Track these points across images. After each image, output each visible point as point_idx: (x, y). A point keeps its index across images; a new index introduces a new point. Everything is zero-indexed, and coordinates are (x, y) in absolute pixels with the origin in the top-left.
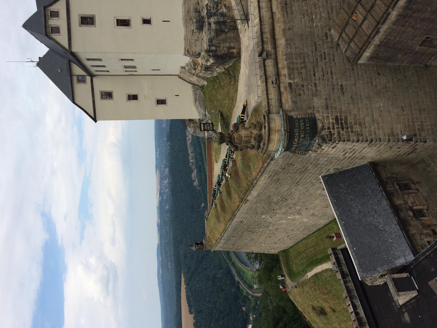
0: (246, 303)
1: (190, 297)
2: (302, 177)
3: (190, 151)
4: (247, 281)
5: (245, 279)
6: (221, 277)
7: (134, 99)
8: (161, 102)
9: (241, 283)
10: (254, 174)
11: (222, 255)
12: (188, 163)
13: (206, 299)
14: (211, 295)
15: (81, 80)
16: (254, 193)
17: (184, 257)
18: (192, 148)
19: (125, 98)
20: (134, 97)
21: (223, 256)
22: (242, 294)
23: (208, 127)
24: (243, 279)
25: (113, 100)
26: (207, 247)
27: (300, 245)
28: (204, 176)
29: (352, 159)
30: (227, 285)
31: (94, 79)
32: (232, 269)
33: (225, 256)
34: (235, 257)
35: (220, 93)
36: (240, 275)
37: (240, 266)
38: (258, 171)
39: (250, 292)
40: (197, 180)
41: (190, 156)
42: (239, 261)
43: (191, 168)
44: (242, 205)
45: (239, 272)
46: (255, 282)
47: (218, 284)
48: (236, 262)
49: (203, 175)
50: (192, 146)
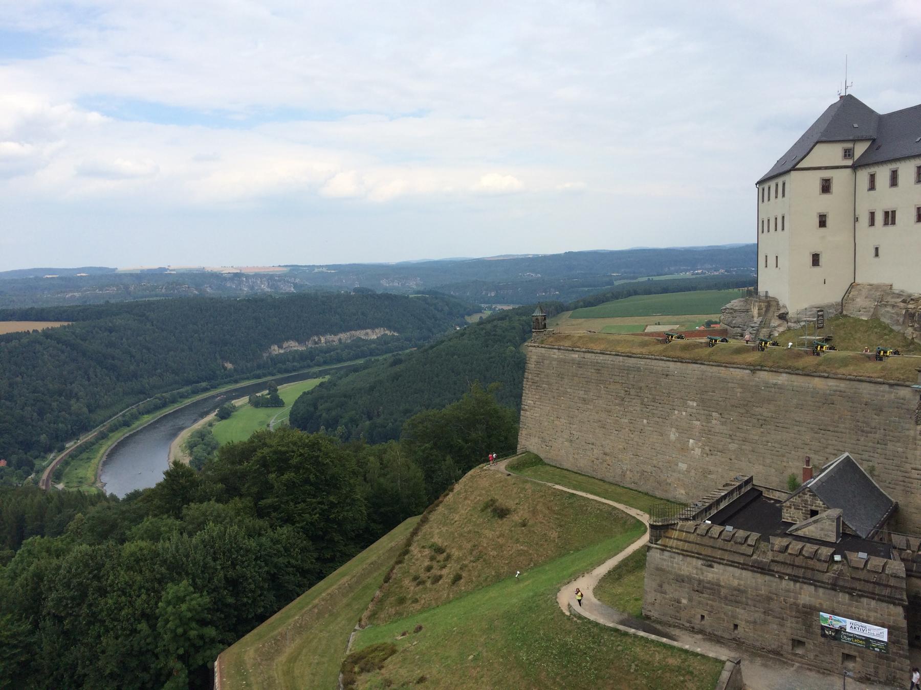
0: (19, 466)
1: (20, 341)
2: (841, 432)
3: (343, 336)
4: (69, 468)
5: (72, 464)
6: (70, 409)
7: (820, 222)
8: (816, 260)
9: (63, 455)
10: (842, 370)
11: (121, 411)
12: (317, 334)
13: (18, 376)
14: (28, 389)
15: (848, 154)
16: (782, 379)
17: (110, 327)
18: (349, 341)
19: (823, 211)
20: (823, 223)
21: (117, 413)
22: (36, 457)
23: (820, 322)
24: (73, 459)
25: (820, 194)
26: (542, 334)
27: (580, 477)
28: (294, 366)
29: (904, 481)
30: (54, 423)
31: (849, 171)
32: (90, 433)
33: (120, 418)
34: (119, 441)
35: (869, 335)
36: (81, 453)
37: (102, 451)
38: (855, 374)
39: (45, 476)
40: (282, 351)
41: (333, 336)
42: (112, 447)
43: (308, 339)
44: (732, 367)
45: (88, 448)
46: (70, 485)
47: (55, 404)
48: (109, 443)
49: (295, 364)
50: (353, 341)
